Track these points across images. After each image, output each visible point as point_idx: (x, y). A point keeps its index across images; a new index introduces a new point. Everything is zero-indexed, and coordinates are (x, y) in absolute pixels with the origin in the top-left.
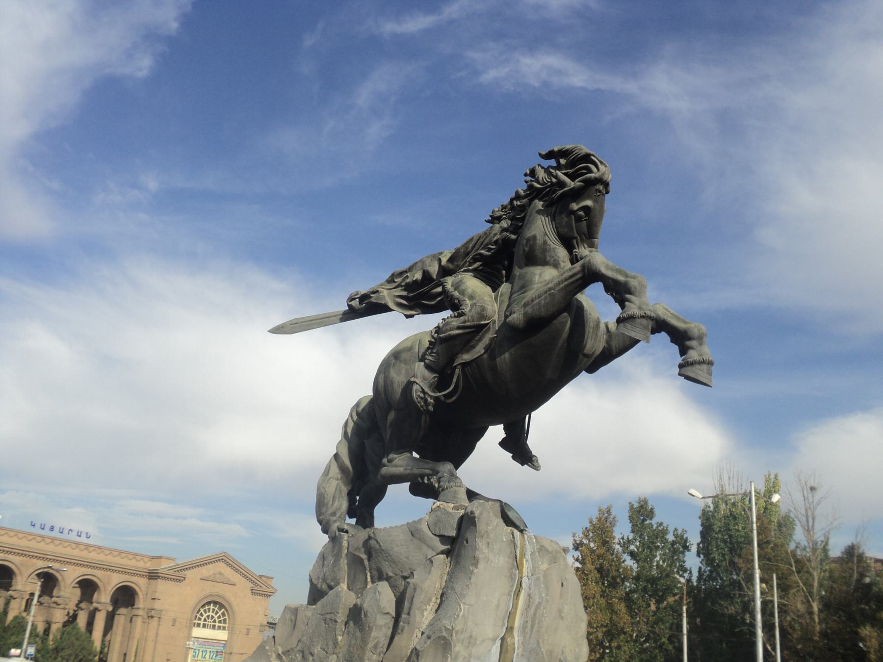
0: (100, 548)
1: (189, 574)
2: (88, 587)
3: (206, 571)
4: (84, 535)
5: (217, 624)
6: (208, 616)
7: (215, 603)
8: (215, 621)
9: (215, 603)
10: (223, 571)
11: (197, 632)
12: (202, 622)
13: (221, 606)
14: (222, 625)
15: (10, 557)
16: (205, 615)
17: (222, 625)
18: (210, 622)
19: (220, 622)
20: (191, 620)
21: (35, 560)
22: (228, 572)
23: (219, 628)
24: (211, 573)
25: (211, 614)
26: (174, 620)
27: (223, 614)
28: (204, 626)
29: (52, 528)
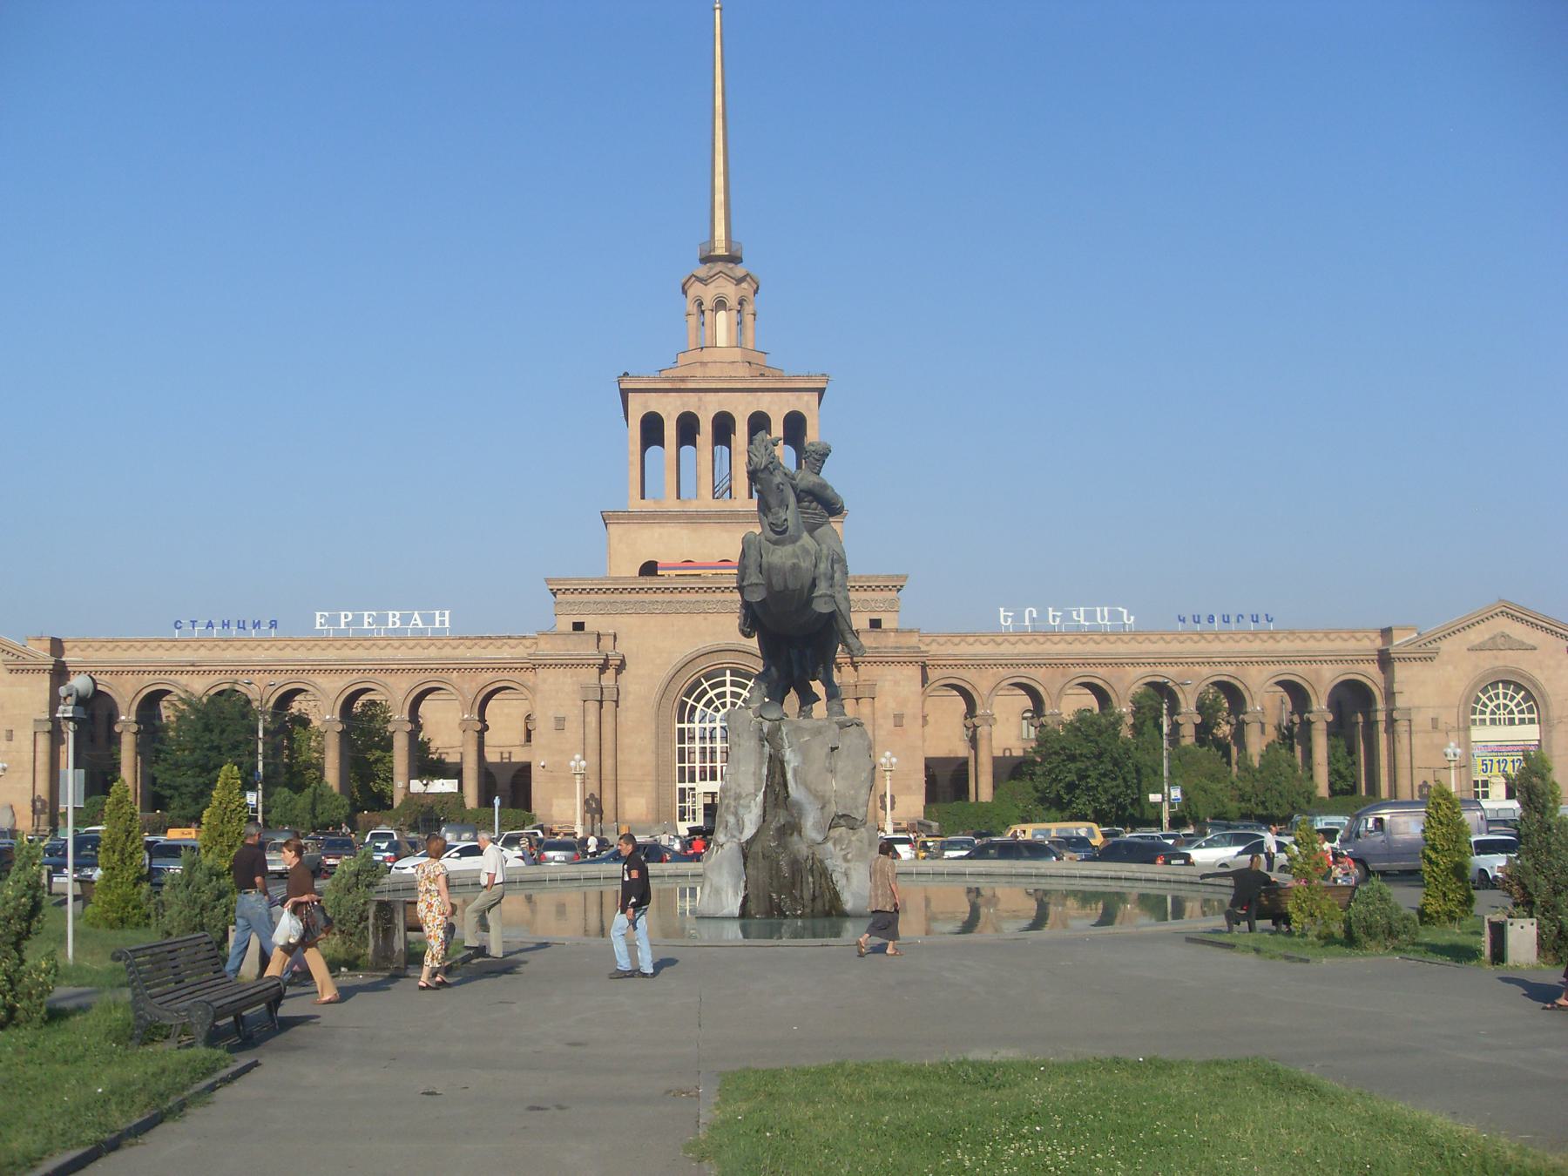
0: (1292, 633)
1: (1445, 645)
2: (1297, 693)
3: (1475, 636)
4: (1263, 621)
5: (1517, 716)
6: (1497, 706)
7: (1506, 683)
8: (1511, 712)
9: (1506, 683)
10: (1507, 631)
11: (1477, 734)
12: (1487, 717)
13: (1519, 687)
14: (1526, 716)
15: (1161, 670)
16: (1491, 706)
17: (1526, 716)
18: (1502, 714)
19: (1521, 712)
20: (1466, 719)
21: (1197, 667)
22: (1518, 631)
23: (1522, 721)
24: (1487, 637)
25: (1501, 701)
26: (1435, 721)
27: (1525, 699)
28: (1493, 722)
29: (1211, 619)
